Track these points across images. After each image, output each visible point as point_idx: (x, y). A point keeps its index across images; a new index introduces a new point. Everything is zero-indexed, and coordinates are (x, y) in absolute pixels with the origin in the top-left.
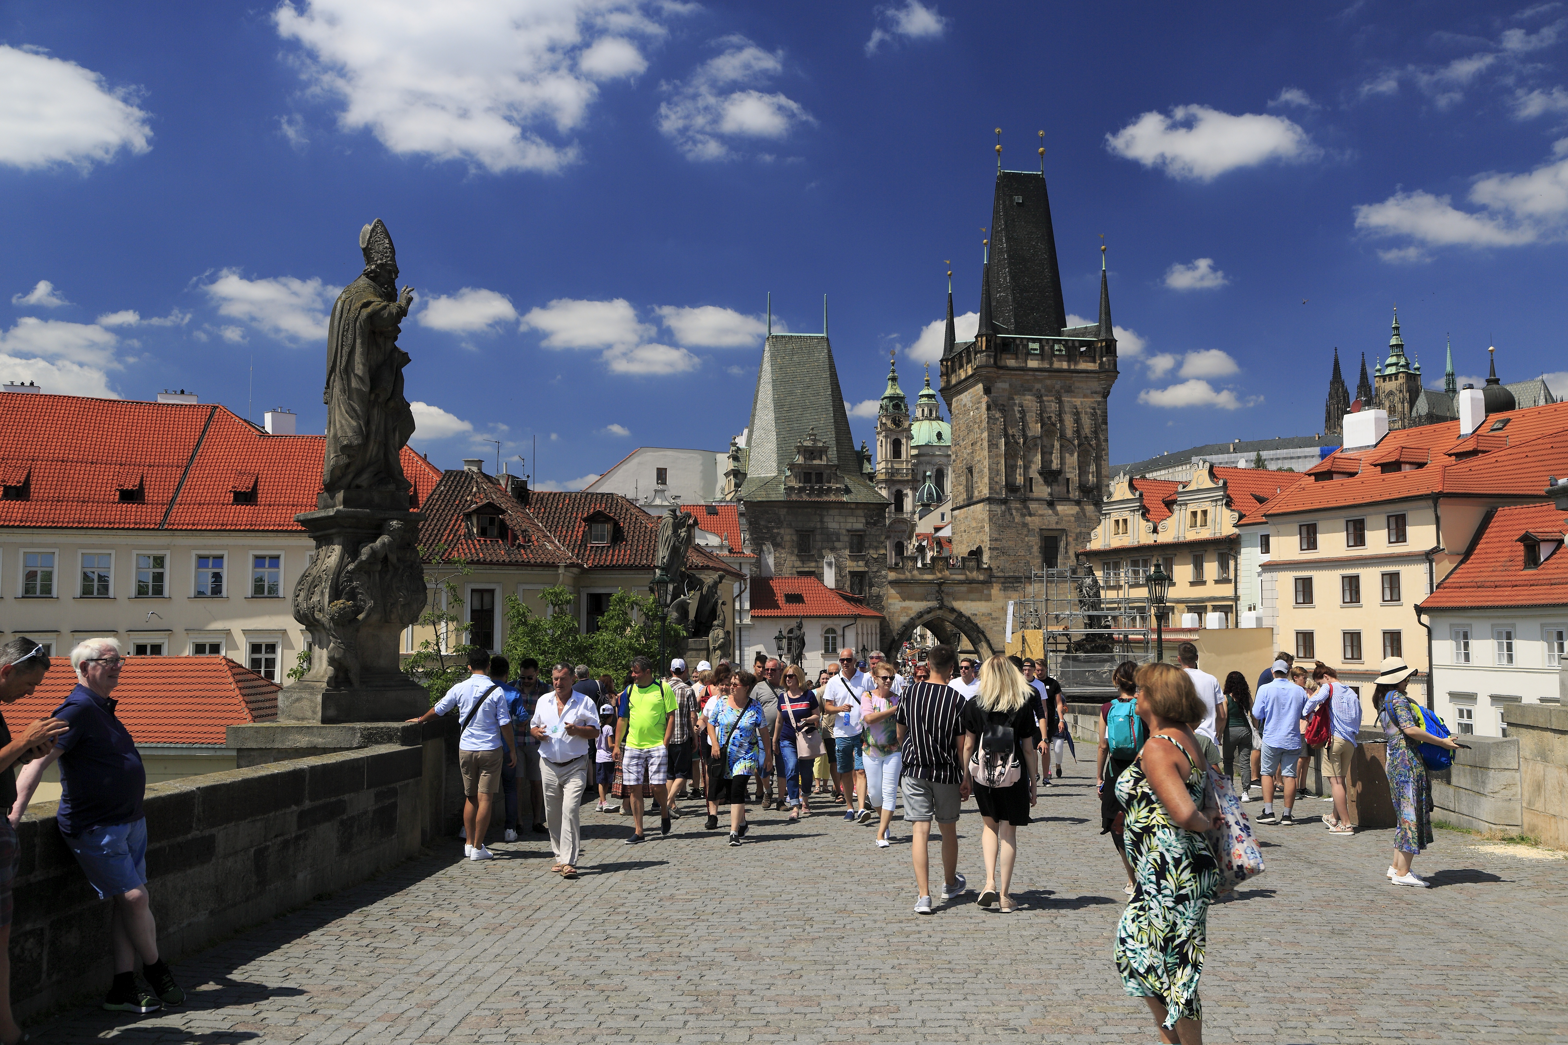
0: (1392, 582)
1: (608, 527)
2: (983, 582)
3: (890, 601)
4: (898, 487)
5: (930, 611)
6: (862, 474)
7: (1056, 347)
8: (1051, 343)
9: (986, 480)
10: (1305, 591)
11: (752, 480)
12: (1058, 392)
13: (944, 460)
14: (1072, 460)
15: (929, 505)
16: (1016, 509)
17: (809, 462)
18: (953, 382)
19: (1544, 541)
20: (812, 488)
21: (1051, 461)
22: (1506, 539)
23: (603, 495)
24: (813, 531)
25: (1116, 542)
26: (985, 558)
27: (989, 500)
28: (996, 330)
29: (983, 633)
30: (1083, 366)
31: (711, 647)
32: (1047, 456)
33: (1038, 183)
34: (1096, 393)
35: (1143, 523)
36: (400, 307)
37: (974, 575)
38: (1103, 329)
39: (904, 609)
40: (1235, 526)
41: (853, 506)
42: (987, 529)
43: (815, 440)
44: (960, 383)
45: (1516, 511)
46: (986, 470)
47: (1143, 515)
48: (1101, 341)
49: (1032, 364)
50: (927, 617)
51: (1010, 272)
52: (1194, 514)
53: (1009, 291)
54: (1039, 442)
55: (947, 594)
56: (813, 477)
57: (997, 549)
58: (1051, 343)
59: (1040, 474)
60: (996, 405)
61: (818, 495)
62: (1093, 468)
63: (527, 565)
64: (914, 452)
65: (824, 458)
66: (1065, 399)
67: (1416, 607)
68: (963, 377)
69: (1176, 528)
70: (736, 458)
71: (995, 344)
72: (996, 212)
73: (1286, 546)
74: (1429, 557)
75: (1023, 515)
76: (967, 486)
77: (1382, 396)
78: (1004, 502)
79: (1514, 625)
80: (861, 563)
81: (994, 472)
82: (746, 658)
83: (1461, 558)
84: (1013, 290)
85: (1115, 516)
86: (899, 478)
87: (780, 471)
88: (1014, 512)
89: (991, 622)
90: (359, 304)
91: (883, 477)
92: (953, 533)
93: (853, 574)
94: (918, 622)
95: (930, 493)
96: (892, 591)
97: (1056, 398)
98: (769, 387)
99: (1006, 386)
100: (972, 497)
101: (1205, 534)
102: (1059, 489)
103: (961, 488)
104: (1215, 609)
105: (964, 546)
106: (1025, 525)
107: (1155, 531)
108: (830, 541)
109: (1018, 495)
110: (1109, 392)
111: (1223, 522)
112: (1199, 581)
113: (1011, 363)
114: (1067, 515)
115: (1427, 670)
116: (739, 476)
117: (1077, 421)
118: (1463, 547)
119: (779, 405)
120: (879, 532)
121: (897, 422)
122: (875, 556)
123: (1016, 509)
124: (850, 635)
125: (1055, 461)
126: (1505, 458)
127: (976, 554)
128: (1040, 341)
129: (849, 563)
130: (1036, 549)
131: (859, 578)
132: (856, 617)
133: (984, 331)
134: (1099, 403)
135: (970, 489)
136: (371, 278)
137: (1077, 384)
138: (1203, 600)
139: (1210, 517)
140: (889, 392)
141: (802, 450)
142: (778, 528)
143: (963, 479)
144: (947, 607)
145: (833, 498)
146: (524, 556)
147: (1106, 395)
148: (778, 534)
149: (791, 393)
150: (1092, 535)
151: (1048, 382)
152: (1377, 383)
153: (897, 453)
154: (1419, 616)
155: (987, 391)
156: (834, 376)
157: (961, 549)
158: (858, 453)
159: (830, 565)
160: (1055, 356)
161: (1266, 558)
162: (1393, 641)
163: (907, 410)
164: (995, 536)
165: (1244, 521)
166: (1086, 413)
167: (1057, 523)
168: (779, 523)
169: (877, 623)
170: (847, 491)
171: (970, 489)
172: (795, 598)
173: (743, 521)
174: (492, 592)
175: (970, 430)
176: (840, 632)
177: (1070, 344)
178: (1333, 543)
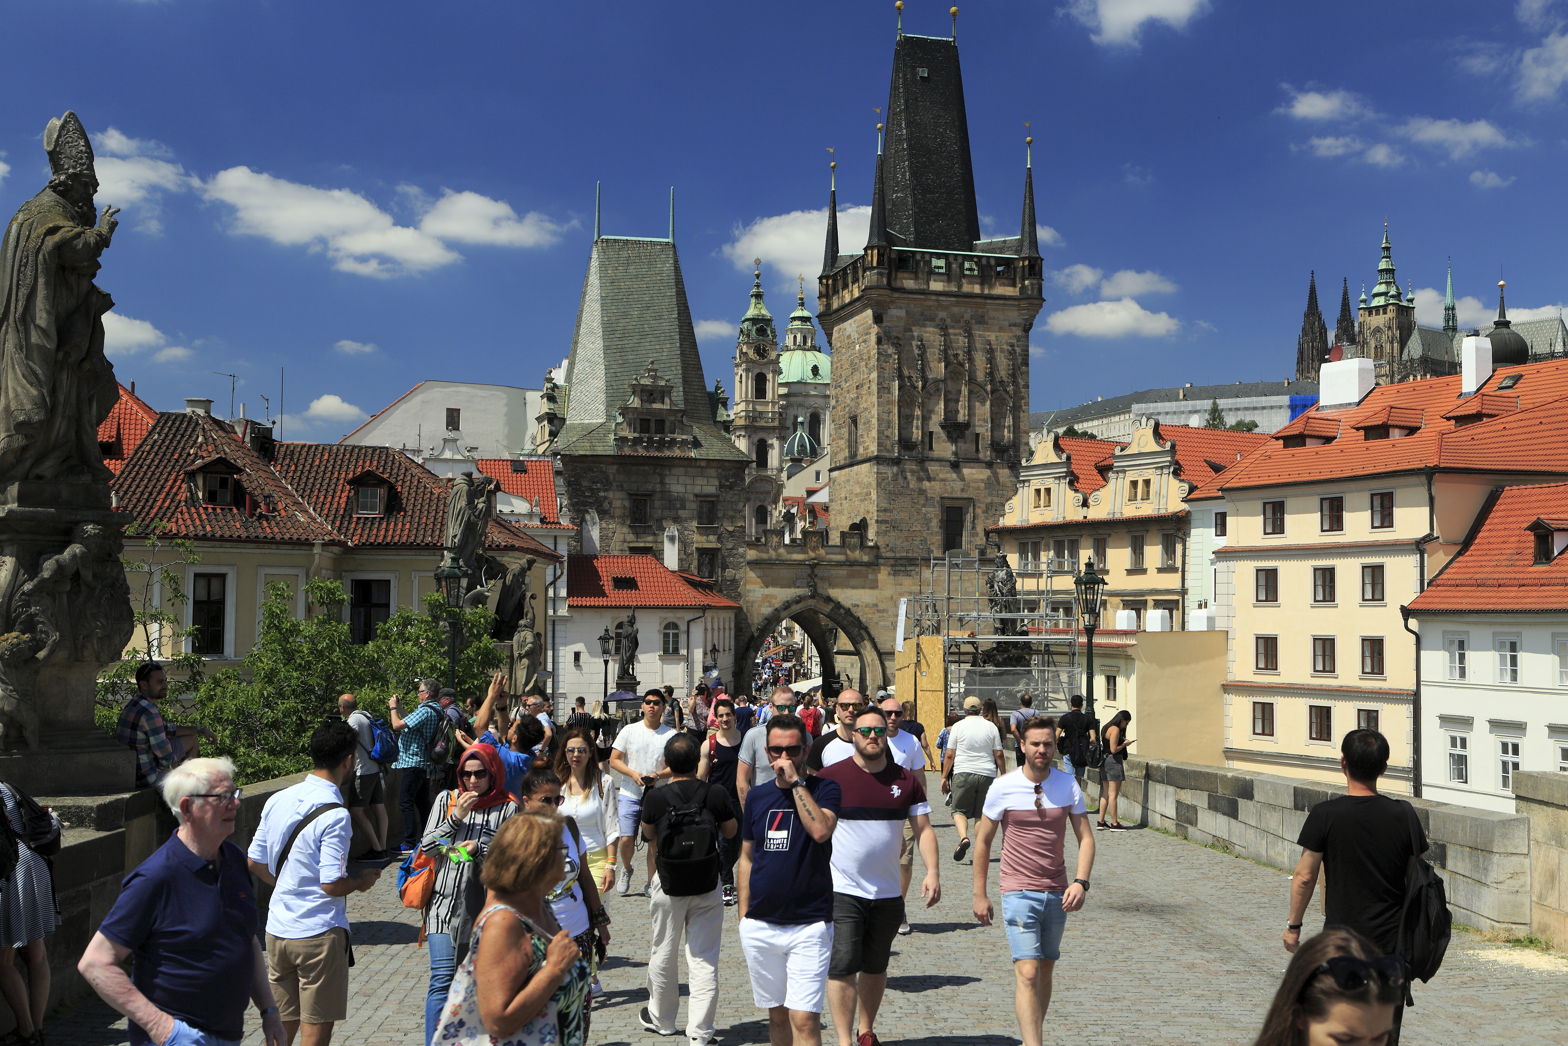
0: (1375, 577)
1: (381, 492)
2: (867, 565)
3: (748, 587)
4: (761, 435)
5: (799, 600)
6: (715, 422)
7: (967, 265)
8: (960, 260)
9: (874, 433)
10: (1268, 586)
11: (573, 427)
12: (968, 323)
13: (820, 402)
14: (984, 410)
15: (800, 460)
19: (1559, 530)
21: (957, 412)
22: (1514, 526)
23: (374, 449)
24: (650, 495)
25: (1036, 518)
26: (871, 533)
27: (877, 460)
28: (891, 241)
29: (866, 629)
30: (1000, 290)
31: (516, 654)
32: (952, 405)
33: (949, 52)
34: (1015, 325)
35: (1071, 494)
36: (100, 235)
37: (857, 555)
38: (1026, 243)
39: (766, 597)
40: (1185, 500)
41: (703, 464)
42: (874, 496)
43: (655, 378)
44: (843, 307)
45: (1526, 492)
46: (874, 421)
47: (1071, 483)
48: (1024, 259)
49: (936, 286)
50: (796, 608)
51: (910, 167)
52: (1134, 484)
53: (909, 191)
54: (942, 386)
55: (823, 579)
56: (653, 426)
57: (886, 522)
58: (960, 260)
59: (943, 427)
60: (889, 338)
61: (659, 449)
62: (1009, 421)
63: (271, 542)
64: (783, 391)
65: (667, 400)
66: (976, 332)
67: (1403, 609)
68: (847, 299)
69: (1111, 502)
70: (551, 398)
71: (889, 258)
72: (894, 88)
73: (1247, 528)
74: (1420, 546)
75: (920, 480)
76: (849, 441)
77: (1367, 333)
78: (897, 462)
79: (1519, 634)
80: (712, 538)
81: (884, 423)
82: (561, 660)
83: (1458, 548)
84: (914, 189)
85: (1036, 484)
86: (762, 423)
87: (610, 417)
88: (909, 475)
89: (877, 615)
90: (42, 230)
91: (742, 422)
92: (831, 500)
93: (702, 551)
94: (783, 614)
95: (802, 445)
96: (752, 575)
97: (966, 331)
98: (597, 306)
99: (902, 313)
100: (855, 455)
101: (1146, 510)
102: (966, 447)
103: (843, 443)
104: (1158, 604)
105: (844, 518)
106: (922, 492)
107: (1085, 504)
108: (673, 508)
109: (914, 453)
110: (1031, 325)
111: (1169, 496)
112: (1137, 569)
113: (910, 284)
114: (975, 481)
115: (1414, 688)
116: (556, 422)
117: (991, 360)
118: (1461, 534)
119: (609, 330)
120: (735, 498)
121: (761, 352)
122: (731, 529)
123: (913, 472)
124: (697, 631)
125: (961, 412)
126: (1515, 425)
127: (860, 527)
128: (946, 256)
129: (696, 537)
130: (935, 523)
131: (708, 557)
132: (704, 608)
133: (875, 241)
135: (853, 444)
136: (60, 193)
137: (992, 314)
138: (1142, 593)
140: (751, 312)
141: (638, 389)
142: (606, 490)
143: (845, 431)
144: (821, 596)
145: (677, 452)
146: (267, 530)
147: (1027, 328)
148: (605, 498)
149: (625, 315)
150: (1007, 507)
151: (956, 310)
152: (1359, 317)
153: (760, 392)
154: (1406, 621)
155: (878, 319)
156: (681, 293)
157: (839, 522)
158: (710, 395)
159: (672, 539)
160: (965, 276)
161: (1222, 542)
162: (1374, 649)
163: (775, 336)
164: (884, 505)
165: (1195, 495)
166: (1002, 351)
167: (962, 490)
168: (607, 485)
169: (731, 615)
170: (696, 444)
171: (853, 444)
172: (626, 583)
173: (560, 481)
174: (223, 577)
175: (855, 369)
176: (683, 627)
177: (984, 261)
178: (1304, 526)
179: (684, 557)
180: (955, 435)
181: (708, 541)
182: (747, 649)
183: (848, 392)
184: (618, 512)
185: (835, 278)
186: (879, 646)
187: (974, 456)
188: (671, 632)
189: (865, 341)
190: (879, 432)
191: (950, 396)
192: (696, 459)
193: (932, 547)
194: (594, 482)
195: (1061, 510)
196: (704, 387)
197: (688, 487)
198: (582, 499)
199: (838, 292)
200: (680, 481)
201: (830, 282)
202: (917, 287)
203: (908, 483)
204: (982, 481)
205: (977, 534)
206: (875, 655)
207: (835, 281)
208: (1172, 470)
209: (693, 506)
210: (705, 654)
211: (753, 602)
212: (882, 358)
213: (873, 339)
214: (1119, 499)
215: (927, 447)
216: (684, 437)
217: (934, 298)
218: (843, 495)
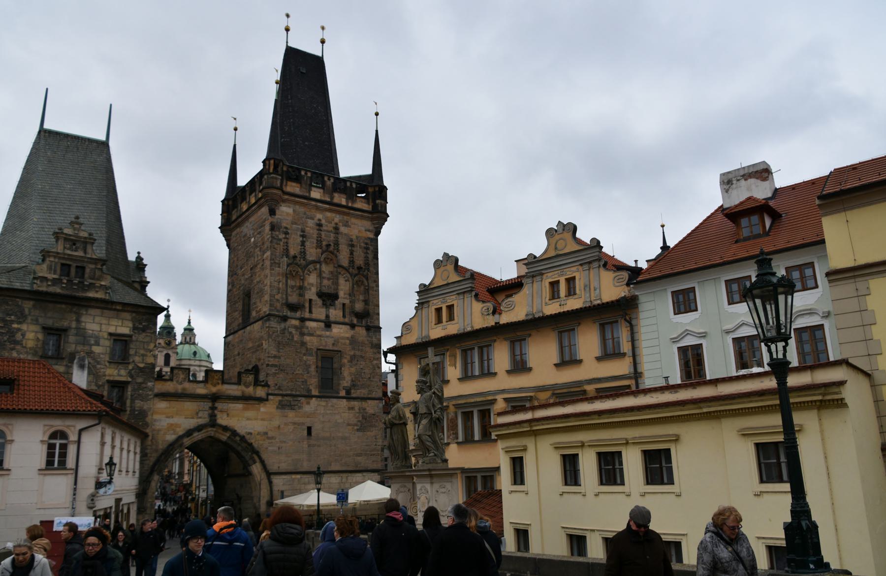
3: (155, 417)
8: (332, 180)
9: (267, 298)
12: (336, 224)
13: (197, 368)
16: (296, 327)
17: (69, 252)
18: (234, 217)
20: (70, 281)
29: (257, 453)
34: (369, 231)
35: (477, 307)
39: (172, 427)
41: (118, 308)
46: (267, 288)
47: (476, 296)
50: (197, 436)
56: (73, 271)
57: (275, 366)
64: (178, 363)
68: (245, 207)
75: (302, 334)
76: (243, 311)
80: (123, 372)
99: (290, 211)
101: (574, 304)
106: (303, 344)
109: (298, 314)
114: (343, 338)
120: (148, 339)
122: (142, 365)
130: (313, 369)
137: (353, 220)
138: (580, 383)
139: (579, 285)
143: (239, 305)
144: (221, 426)
147: (378, 233)
148: (19, 330)
151: (329, 214)
158: (132, 262)
159: (82, 367)
163: (175, 336)
164: (274, 352)
167: (333, 344)
168: (22, 318)
175: (249, 255)
176: (73, 437)
181: (119, 375)
182: (152, 471)
183: (243, 275)
184: (30, 344)
185: (234, 200)
186: (269, 468)
187: (342, 320)
188: (58, 442)
189: (259, 233)
190: (272, 296)
191: (324, 275)
192: (113, 303)
193: (311, 387)
194: (8, 315)
195: (468, 321)
196: (127, 257)
197: (104, 327)
199: (237, 207)
201: (231, 203)
202: (301, 193)
203: (293, 337)
204: (348, 338)
205: (344, 378)
206: (264, 475)
207: (234, 200)
208: (602, 263)
209: (107, 343)
210: (100, 469)
211: (159, 430)
213: (267, 228)
214: (537, 301)
215: (307, 310)
216: (103, 283)
217: (313, 203)
218: (236, 353)
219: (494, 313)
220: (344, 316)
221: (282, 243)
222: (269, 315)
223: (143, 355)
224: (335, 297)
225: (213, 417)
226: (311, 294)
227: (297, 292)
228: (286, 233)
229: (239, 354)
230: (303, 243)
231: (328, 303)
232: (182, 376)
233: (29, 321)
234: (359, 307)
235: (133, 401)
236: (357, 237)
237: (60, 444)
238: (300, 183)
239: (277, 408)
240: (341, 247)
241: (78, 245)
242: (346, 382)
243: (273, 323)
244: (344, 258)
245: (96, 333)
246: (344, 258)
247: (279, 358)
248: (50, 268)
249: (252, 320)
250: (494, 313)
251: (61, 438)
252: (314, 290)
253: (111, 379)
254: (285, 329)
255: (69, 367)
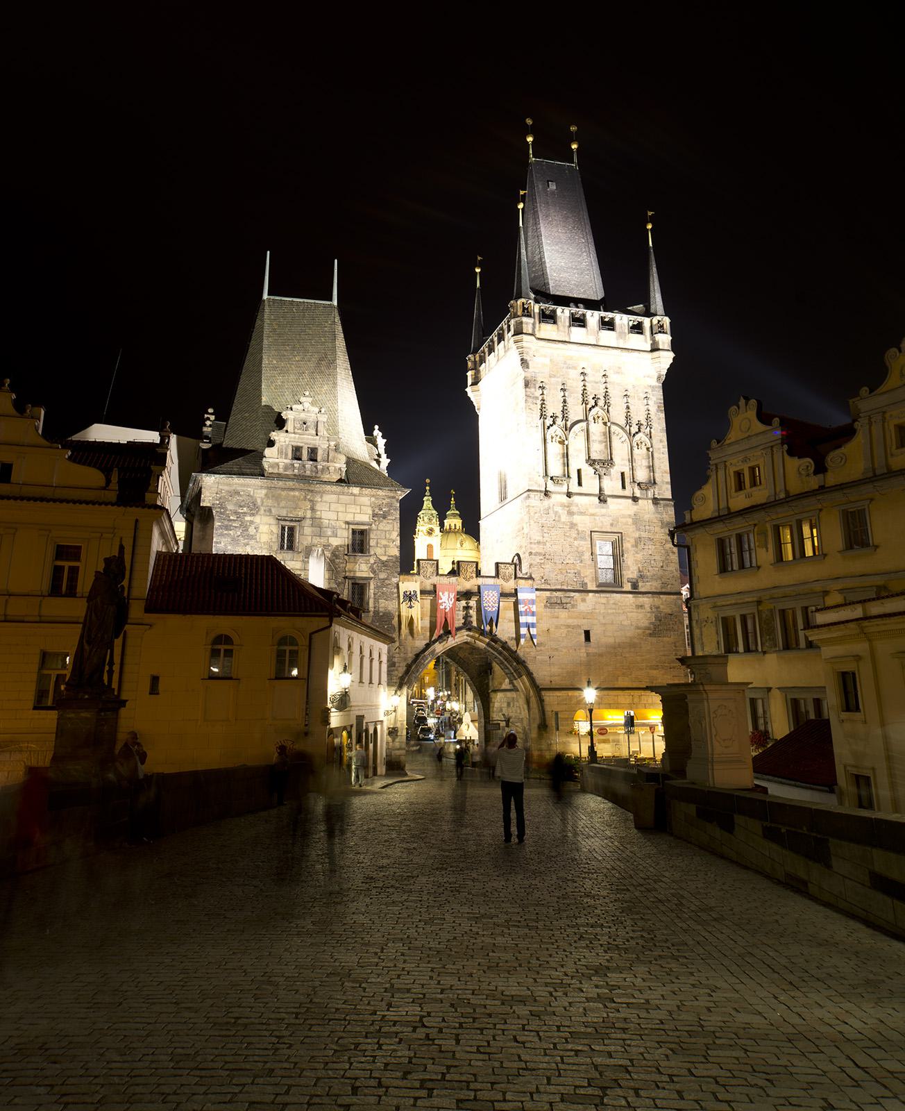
16: (563, 505)
24: (300, 520)
57: (540, 554)
59: (590, 465)
99: (547, 361)
100: (505, 498)
106: (573, 525)
107: (820, 469)
114: (624, 516)
122: (384, 558)
134: (653, 388)
142: (253, 515)
148: (252, 522)
164: (538, 537)
167: (612, 525)
168: (254, 508)
179: (334, 586)
180: (602, 471)
187: (621, 493)
188: (288, 648)
198: (226, 523)
200: (332, 508)
201: (477, 359)
203: (559, 517)
205: (628, 568)
212: (530, 400)
216: (338, 465)
219: (816, 472)
220: (624, 487)
221: (539, 402)
222: (529, 490)
223: (385, 546)
224: (609, 462)
225: (467, 617)
226: (578, 461)
227: (561, 461)
228: (542, 388)
229: (497, 541)
230: (565, 401)
231: (602, 471)
232: (431, 570)
233: (262, 512)
234: (642, 475)
235: (376, 600)
236: (634, 387)
237: (290, 651)
238: (555, 323)
239: (546, 606)
240: (612, 401)
241: (308, 424)
242: (630, 572)
243: (536, 501)
244: (618, 415)
245: (331, 522)
246: (618, 415)
247: (544, 544)
248: (280, 452)
249: (509, 498)
250: (816, 472)
251: (291, 644)
252: (584, 457)
253: (352, 575)
254: (549, 508)
255: (306, 562)
